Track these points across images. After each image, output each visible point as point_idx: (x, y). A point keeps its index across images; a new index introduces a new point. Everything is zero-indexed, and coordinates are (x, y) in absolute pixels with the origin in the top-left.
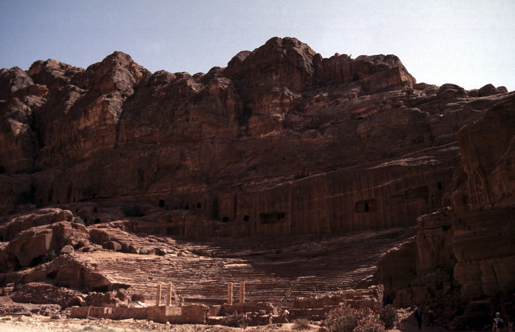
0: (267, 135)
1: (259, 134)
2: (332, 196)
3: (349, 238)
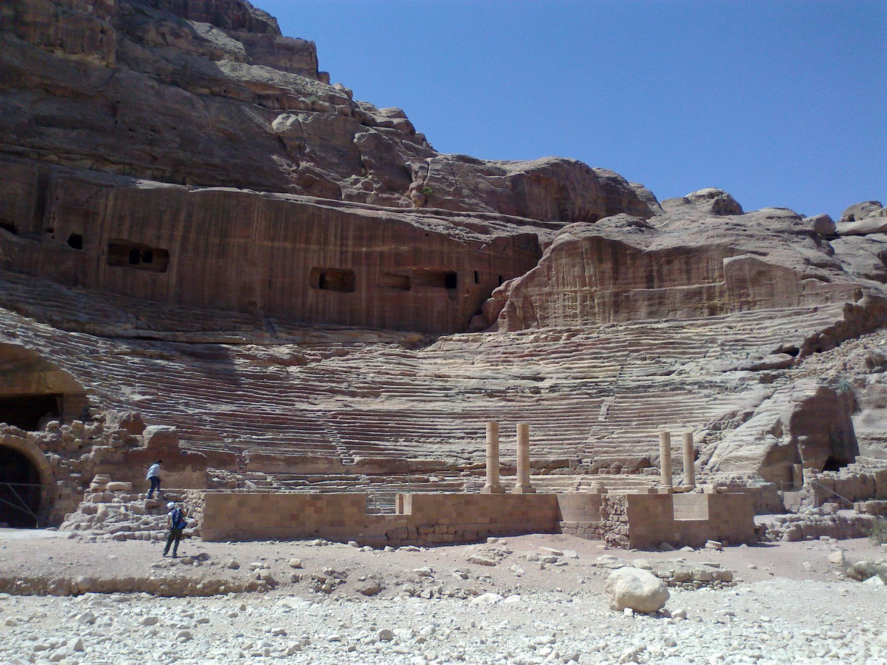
0: (74, 57)
1: (50, 45)
2: (269, 244)
3: (328, 335)
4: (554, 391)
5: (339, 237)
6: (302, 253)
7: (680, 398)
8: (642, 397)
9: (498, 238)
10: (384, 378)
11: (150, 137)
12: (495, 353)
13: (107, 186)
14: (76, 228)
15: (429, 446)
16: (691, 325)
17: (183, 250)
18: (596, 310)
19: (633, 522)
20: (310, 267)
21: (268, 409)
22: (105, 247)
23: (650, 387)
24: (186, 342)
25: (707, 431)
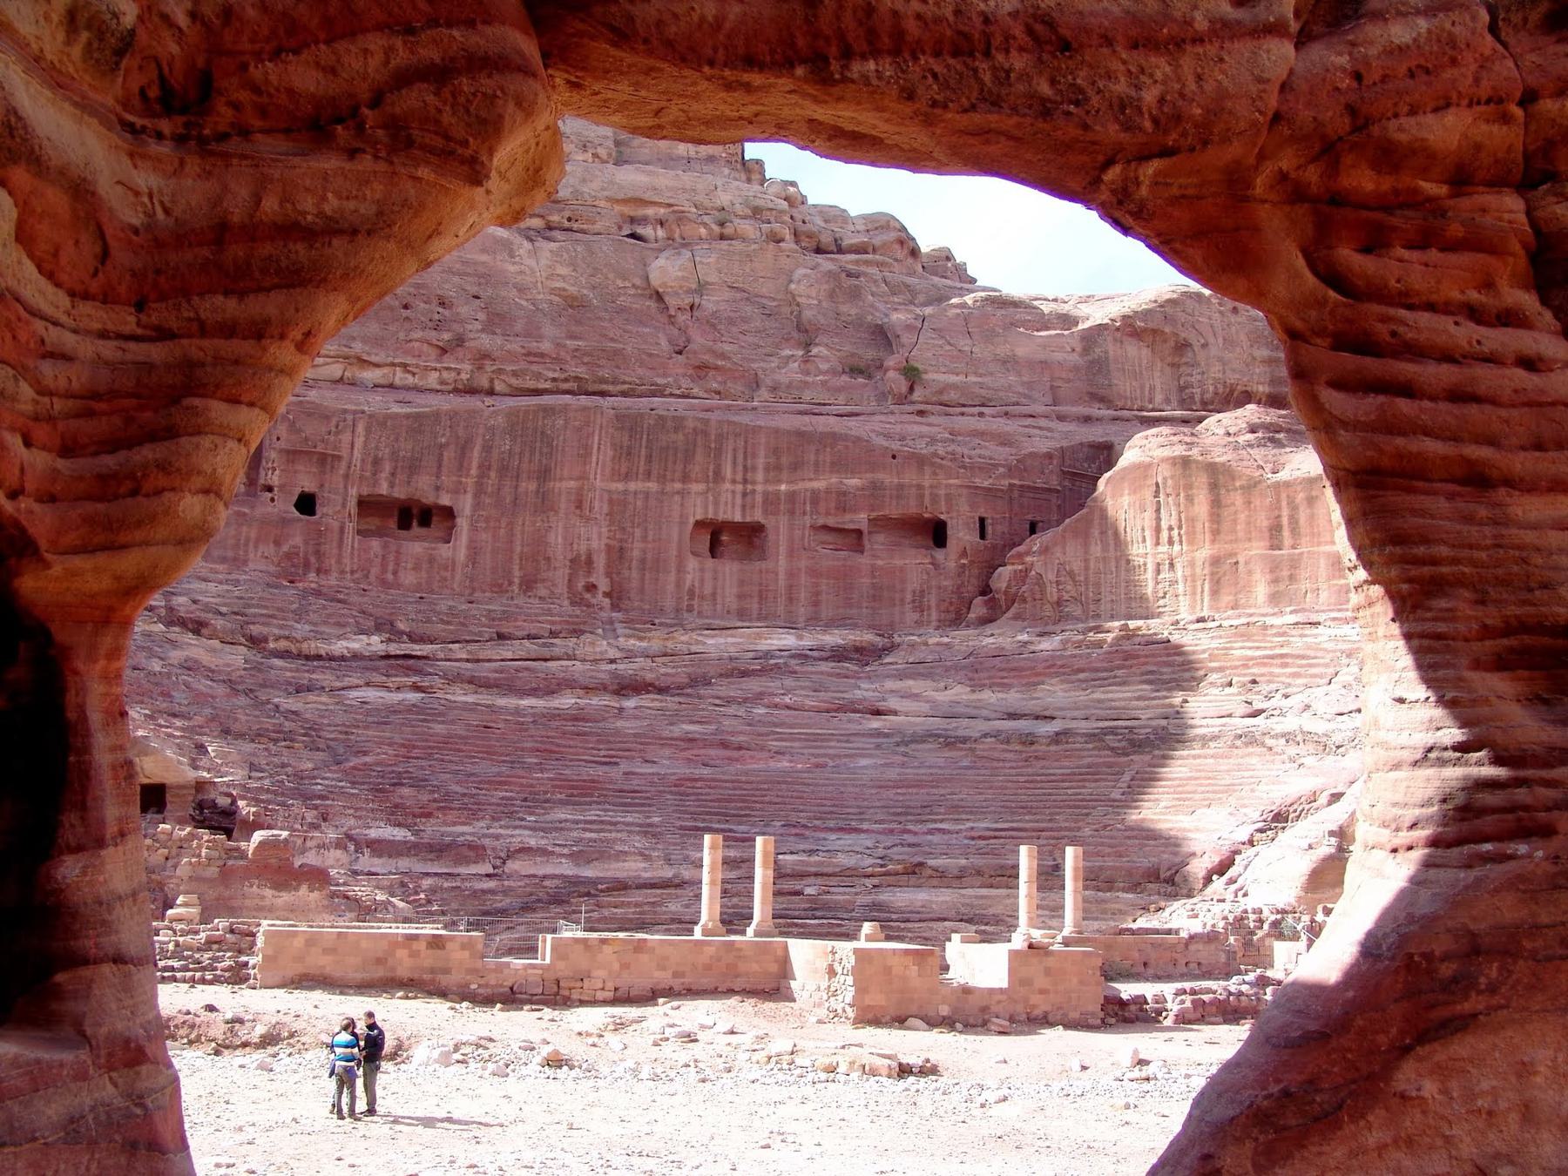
2: (620, 486)
4: (1057, 742)
5: (740, 468)
6: (677, 498)
7: (1254, 760)
8: (1195, 757)
9: (1033, 455)
11: (437, 317)
12: (987, 670)
13: (355, 412)
14: (307, 484)
15: (822, 835)
16: (1334, 619)
17: (477, 505)
18: (1180, 588)
19: (861, 989)
20: (692, 521)
22: (354, 510)
23: (1215, 738)
24: (468, 660)
25: (1261, 825)
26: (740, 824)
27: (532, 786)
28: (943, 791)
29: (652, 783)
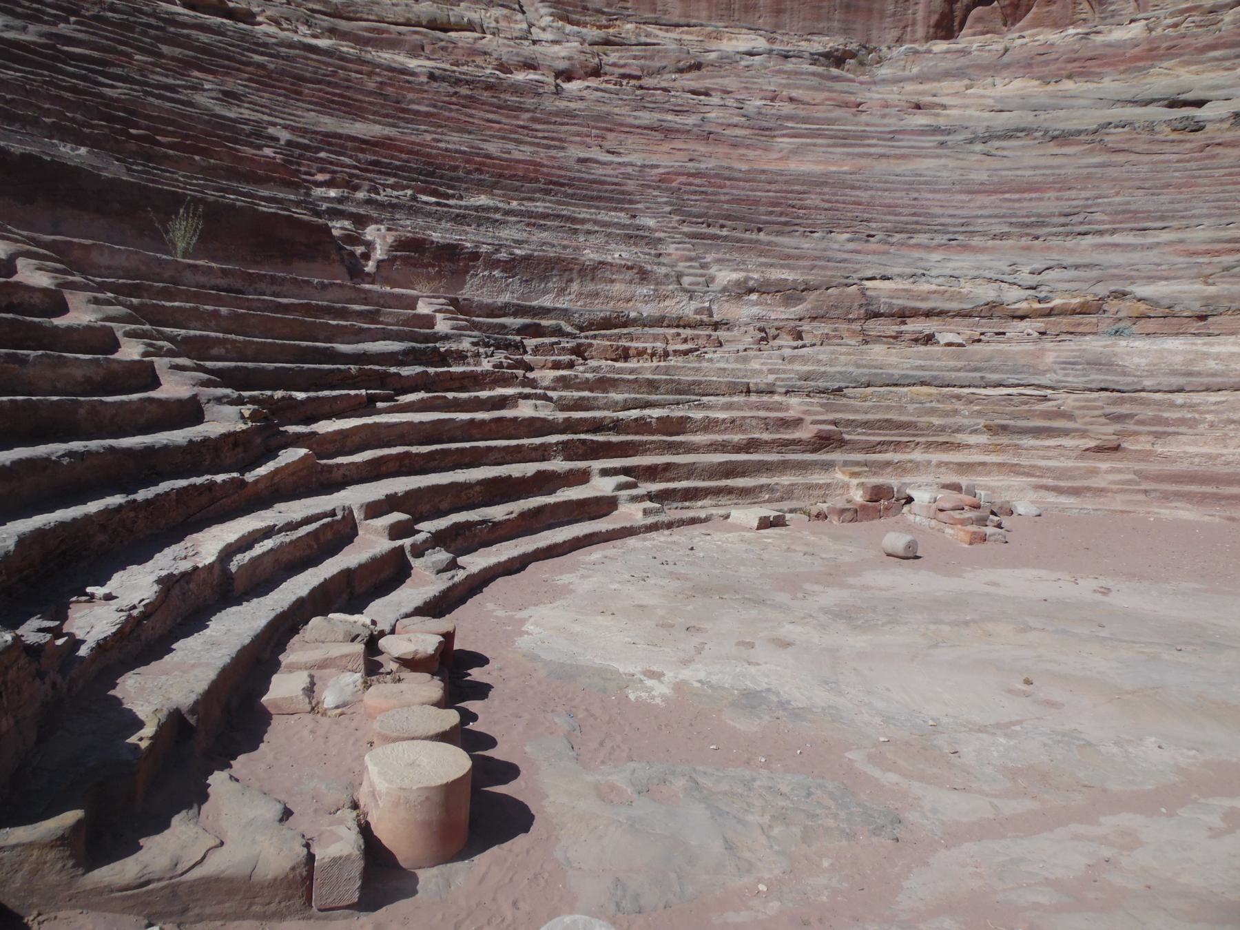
10: (787, 109)
15: (916, 254)
21: (492, 148)
26: (780, 233)
27: (428, 155)
28: (1084, 194)
29: (628, 177)
